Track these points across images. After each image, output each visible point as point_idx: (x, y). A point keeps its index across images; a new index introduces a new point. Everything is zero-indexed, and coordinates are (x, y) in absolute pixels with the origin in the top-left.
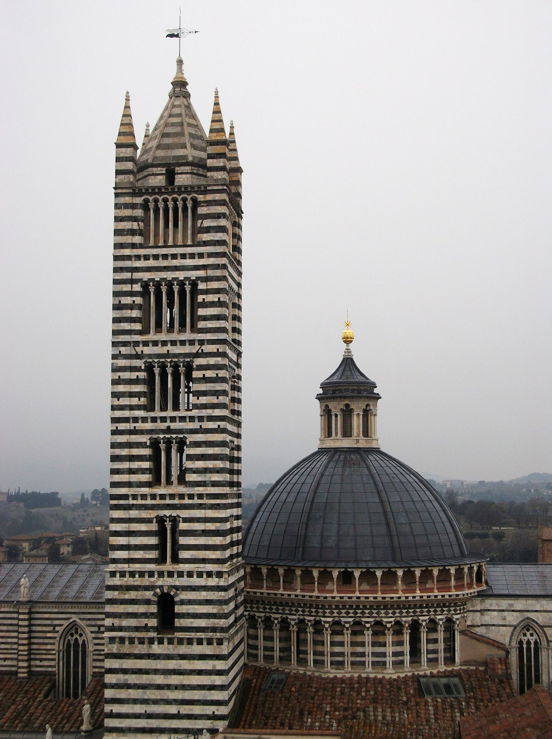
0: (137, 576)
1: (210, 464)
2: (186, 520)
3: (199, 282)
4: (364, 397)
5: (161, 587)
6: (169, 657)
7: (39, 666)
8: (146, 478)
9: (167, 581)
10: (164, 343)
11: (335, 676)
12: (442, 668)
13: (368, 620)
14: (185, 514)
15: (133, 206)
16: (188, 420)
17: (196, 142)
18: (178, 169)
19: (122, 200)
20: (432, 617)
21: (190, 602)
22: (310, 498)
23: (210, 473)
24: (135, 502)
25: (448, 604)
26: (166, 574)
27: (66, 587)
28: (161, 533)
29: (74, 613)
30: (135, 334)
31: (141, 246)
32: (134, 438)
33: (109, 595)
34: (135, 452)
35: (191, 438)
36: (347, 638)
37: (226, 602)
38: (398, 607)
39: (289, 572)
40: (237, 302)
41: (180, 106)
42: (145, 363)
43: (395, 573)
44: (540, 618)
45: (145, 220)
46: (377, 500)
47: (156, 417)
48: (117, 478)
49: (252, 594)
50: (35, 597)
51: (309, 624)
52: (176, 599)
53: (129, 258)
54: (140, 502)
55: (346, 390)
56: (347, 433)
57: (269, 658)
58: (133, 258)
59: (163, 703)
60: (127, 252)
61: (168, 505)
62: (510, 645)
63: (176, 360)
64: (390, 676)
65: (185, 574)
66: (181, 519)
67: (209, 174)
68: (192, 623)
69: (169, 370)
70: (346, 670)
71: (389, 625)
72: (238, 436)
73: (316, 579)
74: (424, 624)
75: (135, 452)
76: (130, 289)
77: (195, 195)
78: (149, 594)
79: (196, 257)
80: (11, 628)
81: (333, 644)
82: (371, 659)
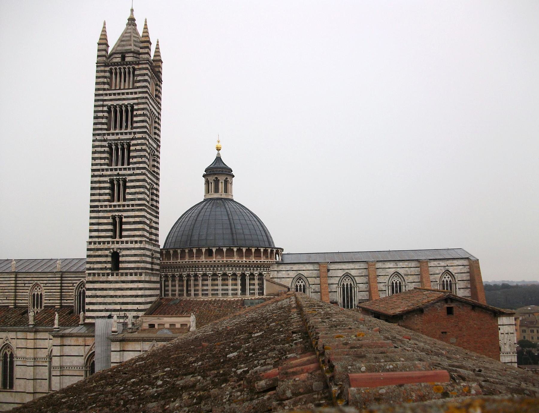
0: (102, 244)
1: (137, 190)
2: (125, 217)
3: (134, 105)
4: (225, 174)
5: (113, 249)
6: (116, 282)
7: (65, 303)
9: (116, 246)
10: (117, 134)
11: (204, 300)
12: (257, 296)
13: (220, 272)
14: (125, 214)
15: (105, 71)
16: (127, 169)
18: (127, 55)
19: (100, 69)
20: (252, 272)
21: (127, 256)
22: (195, 219)
23: (137, 194)
24: (102, 209)
25: (260, 266)
26: (115, 242)
27: (80, 266)
28: (114, 224)
29: (83, 277)
30: (104, 130)
31: (108, 90)
34: (102, 185)
35: (129, 178)
36: (209, 282)
38: (234, 266)
39: (183, 252)
40: (157, 121)
41: (130, 29)
42: (108, 143)
43: (233, 250)
44: (305, 274)
45: (111, 78)
46: (227, 218)
47: (112, 169)
49: (166, 263)
51: (192, 276)
52: (120, 254)
53: (102, 95)
54: (104, 209)
55: (216, 171)
56: (217, 190)
57: (174, 295)
58: (104, 95)
59: (113, 304)
60: (101, 92)
61: (118, 210)
62: (291, 287)
63: (122, 142)
64: (230, 299)
65: (125, 242)
66: (123, 217)
67: (140, 56)
68: (127, 265)
69: (120, 147)
70: (209, 296)
71: (230, 275)
73: (195, 253)
74: (248, 275)
75: (102, 185)
76: (102, 109)
77: (134, 66)
78: (107, 252)
79: (134, 94)
81: (203, 285)
82: (221, 292)
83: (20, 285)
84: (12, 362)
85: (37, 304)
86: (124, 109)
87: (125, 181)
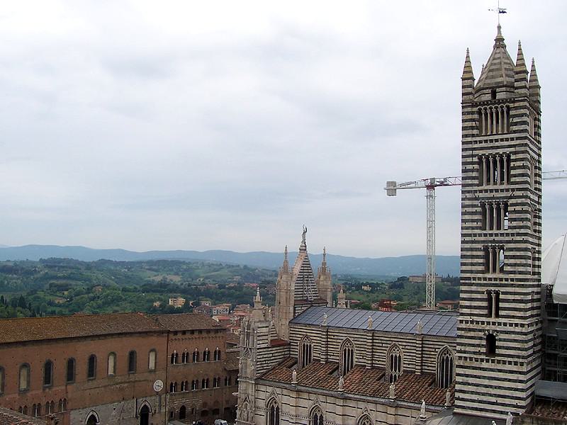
1: (518, 261)
2: (503, 293)
5: (488, 330)
7: (427, 369)
8: (481, 268)
14: (503, 289)
15: (472, 113)
17: (509, 73)
19: (466, 110)
21: (505, 340)
24: (474, 282)
28: (489, 300)
31: (478, 136)
32: (475, 246)
33: (460, 333)
34: (475, 253)
37: (526, 342)
42: (480, 202)
48: (464, 268)
53: (471, 143)
54: (477, 282)
60: (469, 139)
69: (495, 206)
72: (539, 245)
75: (475, 253)
78: (481, 334)
80: (413, 348)
83: (377, 344)
86: (498, 159)
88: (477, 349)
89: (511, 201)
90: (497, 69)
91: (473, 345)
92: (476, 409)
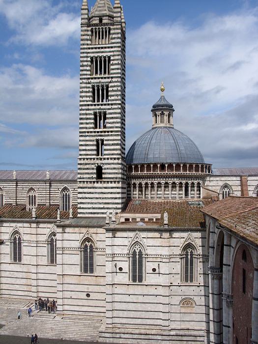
2: (106, 140)
5: (98, 164)
6: (100, 188)
9: (99, 162)
10: (99, 78)
12: (196, 199)
15: (88, 31)
17: (110, 9)
19: (83, 28)
21: (108, 169)
24: (88, 134)
28: (97, 145)
31: (90, 45)
32: (88, 112)
34: (88, 116)
35: (108, 111)
44: (230, 183)
50: (52, 179)
54: (90, 134)
69: (100, 88)
75: (88, 116)
78: (93, 166)
84: (20, 244)
85: (32, 203)
87: (105, 114)
88: (91, 176)
89: (110, 85)
90: (103, 7)
91: (88, 173)
92: (91, 213)
